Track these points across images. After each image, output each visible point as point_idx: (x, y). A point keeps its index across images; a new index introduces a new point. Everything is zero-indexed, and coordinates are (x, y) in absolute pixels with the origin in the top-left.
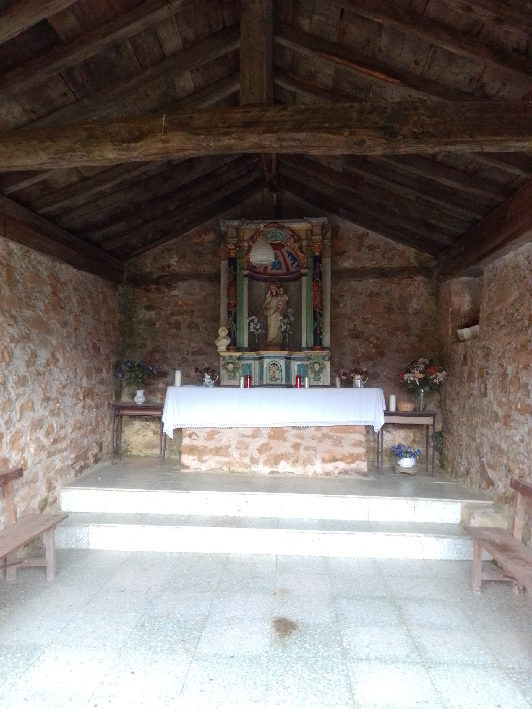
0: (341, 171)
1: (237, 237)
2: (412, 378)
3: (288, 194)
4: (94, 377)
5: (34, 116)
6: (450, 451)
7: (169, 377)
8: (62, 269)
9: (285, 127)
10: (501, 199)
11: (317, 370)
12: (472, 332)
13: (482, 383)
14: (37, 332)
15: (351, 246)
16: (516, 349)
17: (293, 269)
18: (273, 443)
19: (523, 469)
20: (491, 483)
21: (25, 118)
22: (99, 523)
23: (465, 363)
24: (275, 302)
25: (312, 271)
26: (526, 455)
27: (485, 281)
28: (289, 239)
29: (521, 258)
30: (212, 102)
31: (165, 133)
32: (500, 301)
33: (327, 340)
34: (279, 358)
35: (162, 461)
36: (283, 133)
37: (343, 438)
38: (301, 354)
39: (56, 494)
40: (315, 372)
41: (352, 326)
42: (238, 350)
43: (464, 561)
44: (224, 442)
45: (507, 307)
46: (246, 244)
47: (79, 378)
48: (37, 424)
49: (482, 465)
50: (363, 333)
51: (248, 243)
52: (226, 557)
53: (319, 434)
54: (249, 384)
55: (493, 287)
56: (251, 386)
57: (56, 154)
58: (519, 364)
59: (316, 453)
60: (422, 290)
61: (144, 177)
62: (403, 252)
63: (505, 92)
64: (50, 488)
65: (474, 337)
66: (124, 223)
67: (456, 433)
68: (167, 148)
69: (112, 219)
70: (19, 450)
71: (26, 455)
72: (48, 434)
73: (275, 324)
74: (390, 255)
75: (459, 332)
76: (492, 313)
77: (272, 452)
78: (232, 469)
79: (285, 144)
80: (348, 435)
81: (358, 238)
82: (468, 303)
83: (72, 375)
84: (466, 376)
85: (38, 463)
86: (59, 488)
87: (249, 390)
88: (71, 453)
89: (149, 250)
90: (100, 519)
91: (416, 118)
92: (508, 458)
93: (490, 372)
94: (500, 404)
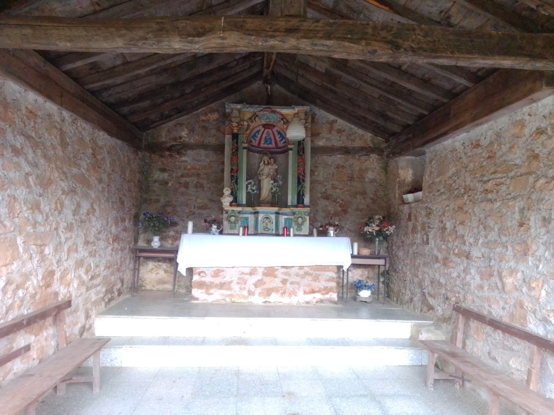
0: (324, 71)
1: (239, 117)
2: (370, 230)
3: (277, 87)
4: (120, 224)
5: (98, 8)
6: (396, 285)
7: (178, 227)
8: (99, 135)
9: (318, 35)
10: (446, 101)
11: (300, 222)
12: (415, 198)
13: (424, 234)
14: (81, 187)
15: (324, 129)
16: (454, 209)
17: (281, 144)
18: (266, 279)
19: (459, 297)
20: (431, 308)
21: (91, 9)
22: (131, 344)
23: (409, 219)
24: (267, 170)
25: (297, 146)
26: (462, 287)
27: (427, 160)
28: (279, 121)
29: (457, 144)
30: (237, 10)
31: (224, 31)
32: (440, 174)
33: (307, 200)
34: (271, 213)
35: (174, 294)
36: (316, 40)
37: (320, 275)
38: (287, 210)
39: (91, 322)
40: (299, 224)
41: (324, 190)
42: (238, 205)
43: (415, 366)
44: (227, 279)
45: (446, 179)
46: (246, 123)
47: (109, 225)
48: (80, 264)
49: (424, 294)
50: (332, 195)
51: (247, 122)
52: (237, 369)
53: (302, 272)
54: (246, 232)
55: (434, 164)
56: (248, 235)
57: (131, 41)
58: (456, 221)
59: (299, 287)
60: (375, 164)
61: (173, 65)
62: (363, 135)
63: (465, 23)
64: (88, 317)
65: (417, 201)
66: (149, 101)
67: (401, 272)
68: (223, 43)
69: (141, 97)
70: (66, 285)
71: (71, 289)
72: (87, 272)
73: (267, 185)
74: (353, 137)
75: (405, 196)
76: (433, 183)
77: (265, 286)
78: (233, 300)
79: (316, 48)
80: (323, 272)
81: (329, 124)
82: (410, 175)
83: (105, 223)
84: (410, 229)
85: (79, 296)
86: (94, 316)
87: (247, 238)
88: (102, 287)
89: (164, 123)
90: (130, 342)
91: (414, 37)
92: (446, 290)
93: (432, 227)
94: (439, 250)
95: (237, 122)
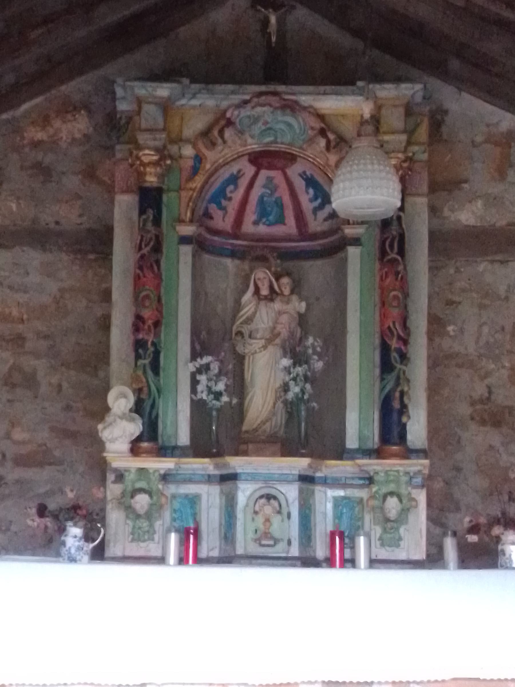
11: (393, 514)
15: (478, 165)
17: (316, 224)
24: (265, 318)
28: (311, 141)
34: (284, 479)
40: (387, 520)
42: (163, 451)
51: (195, 146)
56: (198, 561)
73: (267, 374)
81: (496, 144)
87: (193, 573)
95: (157, 150)
